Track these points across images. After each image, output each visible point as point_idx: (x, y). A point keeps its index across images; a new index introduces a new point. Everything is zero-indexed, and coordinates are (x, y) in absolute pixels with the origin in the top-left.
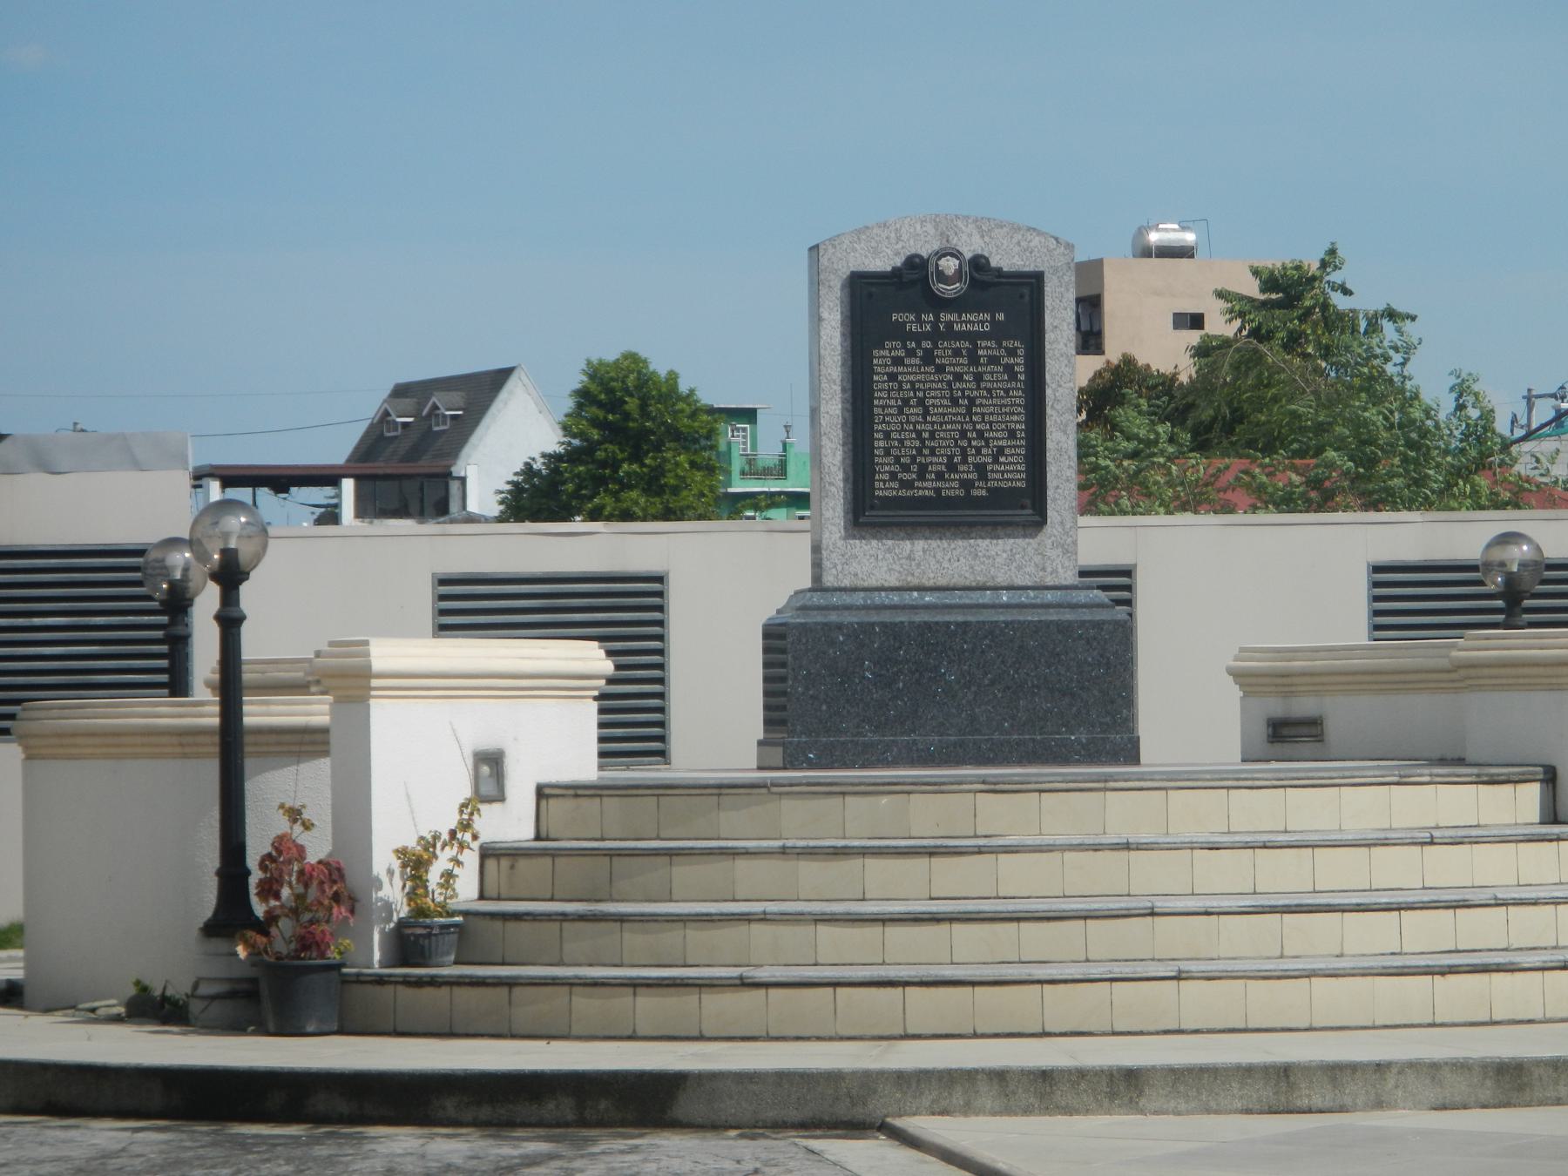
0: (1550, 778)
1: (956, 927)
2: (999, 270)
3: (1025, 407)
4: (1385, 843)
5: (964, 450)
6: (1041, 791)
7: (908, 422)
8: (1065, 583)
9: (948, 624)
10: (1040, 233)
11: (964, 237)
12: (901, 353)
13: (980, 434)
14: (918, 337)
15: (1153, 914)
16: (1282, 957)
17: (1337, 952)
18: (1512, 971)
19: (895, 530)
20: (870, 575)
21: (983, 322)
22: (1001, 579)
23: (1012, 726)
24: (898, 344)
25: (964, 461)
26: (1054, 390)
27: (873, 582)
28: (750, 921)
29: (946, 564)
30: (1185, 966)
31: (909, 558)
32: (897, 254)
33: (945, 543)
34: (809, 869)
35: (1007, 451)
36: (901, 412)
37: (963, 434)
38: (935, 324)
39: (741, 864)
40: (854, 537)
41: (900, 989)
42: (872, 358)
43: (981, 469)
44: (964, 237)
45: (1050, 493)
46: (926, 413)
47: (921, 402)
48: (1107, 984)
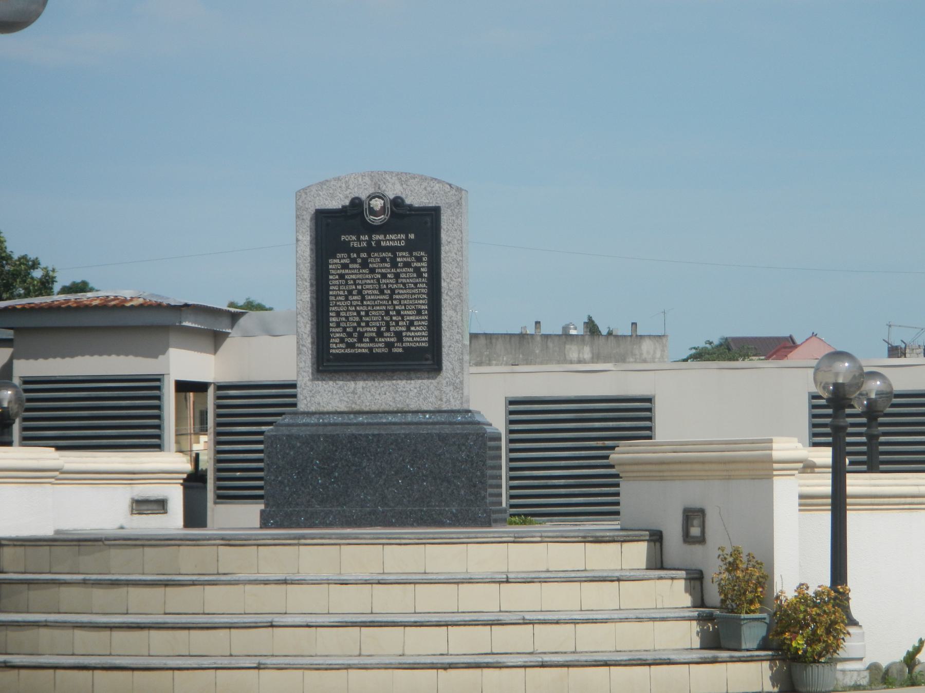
0: (656, 538)
1: (153, 633)
2: (410, 207)
3: (428, 294)
4: (470, 581)
5: (388, 322)
6: (258, 545)
7: (351, 305)
8: (454, 408)
9: (367, 436)
10: (439, 182)
11: (390, 185)
12: (347, 261)
13: (398, 313)
14: (358, 251)
15: (272, 626)
16: (360, 655)
17: (401, 653)
18: (500, 667)
19: (344, 375)
20: (329, 403)
21: (400, 240)
22: (413, 406)
23: (409, 501)
24: (345, 255)
25: (388, 330)
26: (448, 283)
27: (329, 408)
28: (39, 626)
29: (377, 397)
30: (263, 660)
31: (354, 393)
32: (347, 197)
33: (376, 383)
34: (99, 594)
35: (416, 323)
36: (347, 299)
37: (387, 312)
38: (369, 242)
39: (64, 590)
40: (318, 380)
41: (91, 672)
42: (328, 264)
43: (399, 335)
44: (390, 185)
45: (445, 350)
46: (363, 299)
47: (360, 292)
48: (213, 671)
